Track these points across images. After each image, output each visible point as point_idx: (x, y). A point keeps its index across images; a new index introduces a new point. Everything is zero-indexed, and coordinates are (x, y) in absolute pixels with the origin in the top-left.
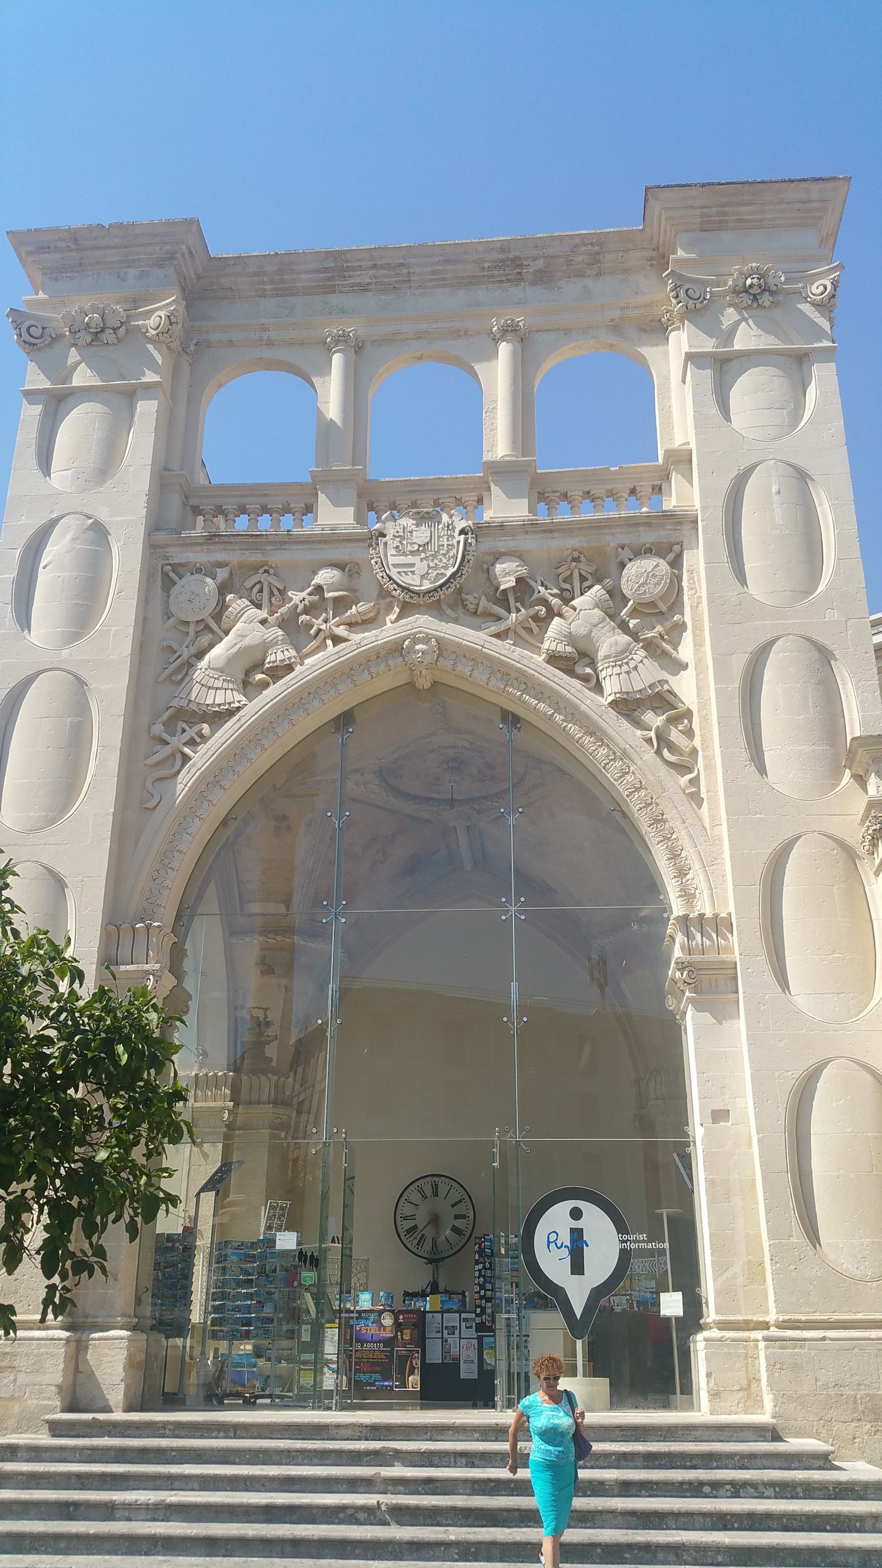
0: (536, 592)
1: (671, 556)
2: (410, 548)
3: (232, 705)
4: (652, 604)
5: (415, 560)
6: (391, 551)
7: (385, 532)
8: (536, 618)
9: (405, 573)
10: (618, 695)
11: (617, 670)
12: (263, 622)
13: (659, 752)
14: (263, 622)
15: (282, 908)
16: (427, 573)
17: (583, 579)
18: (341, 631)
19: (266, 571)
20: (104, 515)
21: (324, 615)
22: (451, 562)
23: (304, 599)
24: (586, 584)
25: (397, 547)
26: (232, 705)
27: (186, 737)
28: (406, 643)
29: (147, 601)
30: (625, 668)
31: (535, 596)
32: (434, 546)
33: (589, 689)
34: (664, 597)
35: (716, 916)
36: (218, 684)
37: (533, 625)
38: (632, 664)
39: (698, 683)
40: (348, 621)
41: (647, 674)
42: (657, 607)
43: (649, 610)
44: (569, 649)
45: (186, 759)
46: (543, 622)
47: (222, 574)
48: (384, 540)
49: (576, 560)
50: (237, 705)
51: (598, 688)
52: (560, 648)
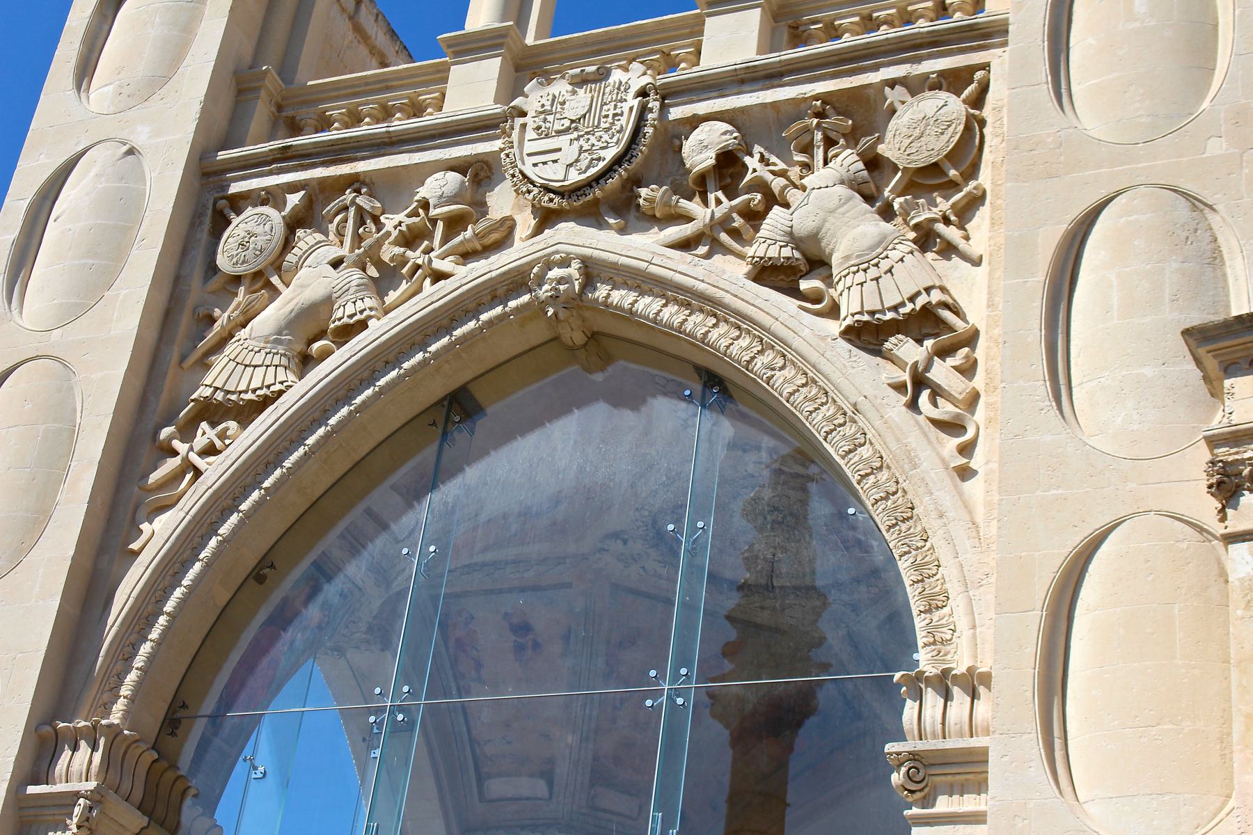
0: (750, 171)
2: (558, 127)
3: (272, 388)
5: (563, 141)
6: (530, 134)
7: (525, 108)
9: (545, 163)
10: (857, 317)
11: (860, 277)
13: (913, 405)
14: (336, 264)
15: (541, 788)
16: (577, 161)
17: (829, 143)
19: (358, 191)
20: (140, 138)
21: (426, 243)
22: (615, 139)
23: (400, 224)
25: (539, 128)
26: (272, 388)
27: (200, 442)
28: (535, 270)
29: (185, 252)
30: (873, 272)
31: (749, 177)
32: (591, 120)
33: (818, 314)
34: (954, 156)
35: (971, 670)
36: (258, 359)
37: (738, 222)
38: (885, 265)
39: (988, 286)
40: (461, 249)
41: (908, 278)
42: (945, 174)
43: (928, 179)
44: (786, 252)
45: (198, 473)
46: (754, 217)
47: (294, 199)
48: (521, 120)
49: (820, 115)
50: (277, 387)
51: (833, 311)
52: (773, 252)
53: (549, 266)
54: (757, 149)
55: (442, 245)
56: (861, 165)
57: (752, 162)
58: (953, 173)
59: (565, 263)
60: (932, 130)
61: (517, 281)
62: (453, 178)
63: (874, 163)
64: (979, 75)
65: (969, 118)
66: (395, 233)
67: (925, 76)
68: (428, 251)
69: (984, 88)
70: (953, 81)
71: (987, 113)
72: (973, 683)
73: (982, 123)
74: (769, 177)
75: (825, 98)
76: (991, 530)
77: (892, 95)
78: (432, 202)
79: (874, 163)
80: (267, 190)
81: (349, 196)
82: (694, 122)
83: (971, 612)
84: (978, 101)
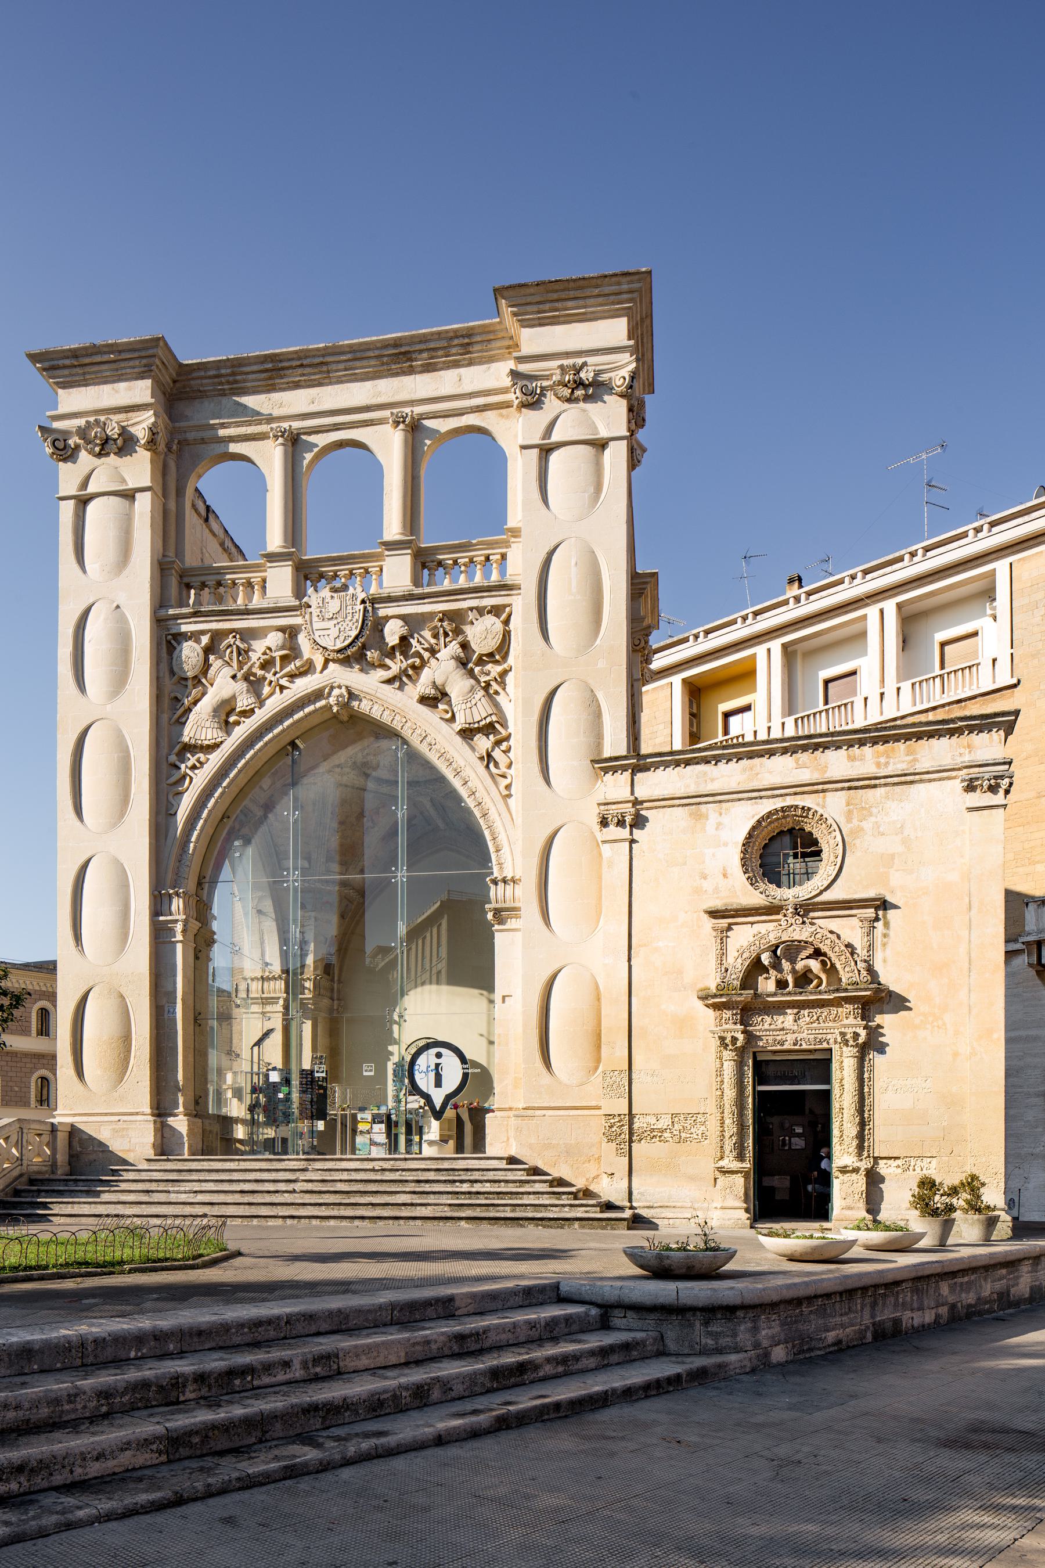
1: (504, 617)
4: (491, 655)
8: (413, 667)
12: (234, 677)
14: (234, 677)
17: (446, 635)
18: (284, 682)
19: (235, 637)
24: (447, 640)
28: (327, 690)
29: (158, 664)
31: (413, 650)
34: (499, 649)
37: (410, 672)
47: (205, 640)
49: (441, 620)
53: (332, 688)
54: (416, 635)
55: (281, 670)
56: (460, 650)
57: (414, 642)
58: (497, 657)
59: (340, 687)
60: (490, 636)
61: (318, 695)
62: (280, 634)
63: (465, 646)
64: (508, 609)
65: (505, 630)
66: (258, 664)
67: (486, 607)
68: (275, 674)
69: (510, 616)
70: (496, 611)
71: (512, 626)
72: (514, 881)
73: (509, 632)
74: (422, 652)
75: (445, 614)
76: (519, 821)
77: (471, 616)
78: (273, 649)
79: (465, 646)
80: (191, 632)
81: (230, 640)
82: (387, 618)
83: (511, 855)
84: (507, 622)
